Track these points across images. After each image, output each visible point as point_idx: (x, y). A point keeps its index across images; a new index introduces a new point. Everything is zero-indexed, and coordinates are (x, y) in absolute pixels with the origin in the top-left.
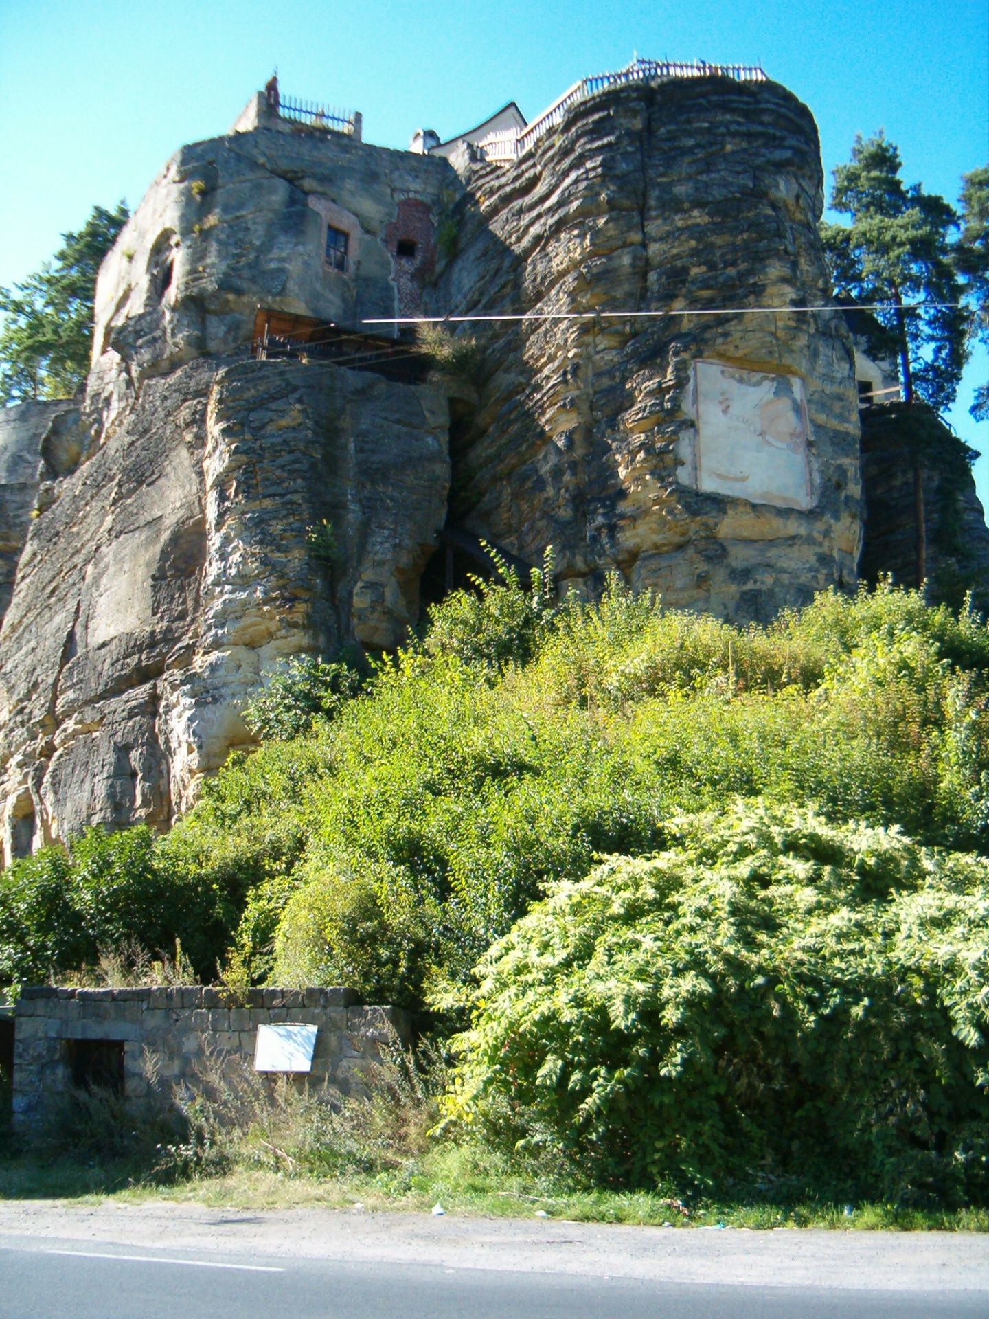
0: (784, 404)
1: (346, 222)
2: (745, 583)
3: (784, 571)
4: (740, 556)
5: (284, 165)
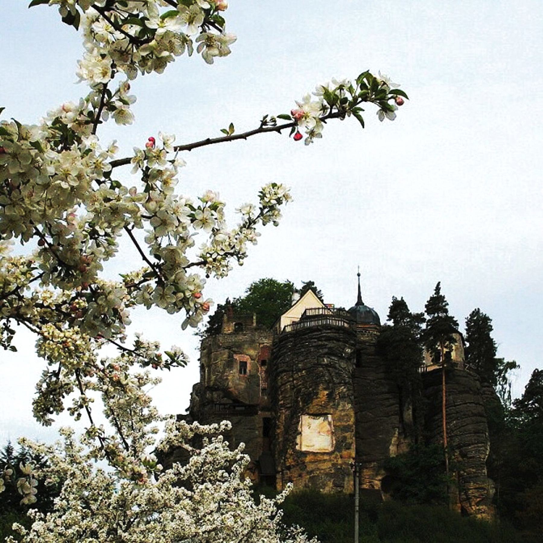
0: (326, 423)
1: (246, 358)
3: (322, 469)
4: (311, 467)
5: (227, 344)
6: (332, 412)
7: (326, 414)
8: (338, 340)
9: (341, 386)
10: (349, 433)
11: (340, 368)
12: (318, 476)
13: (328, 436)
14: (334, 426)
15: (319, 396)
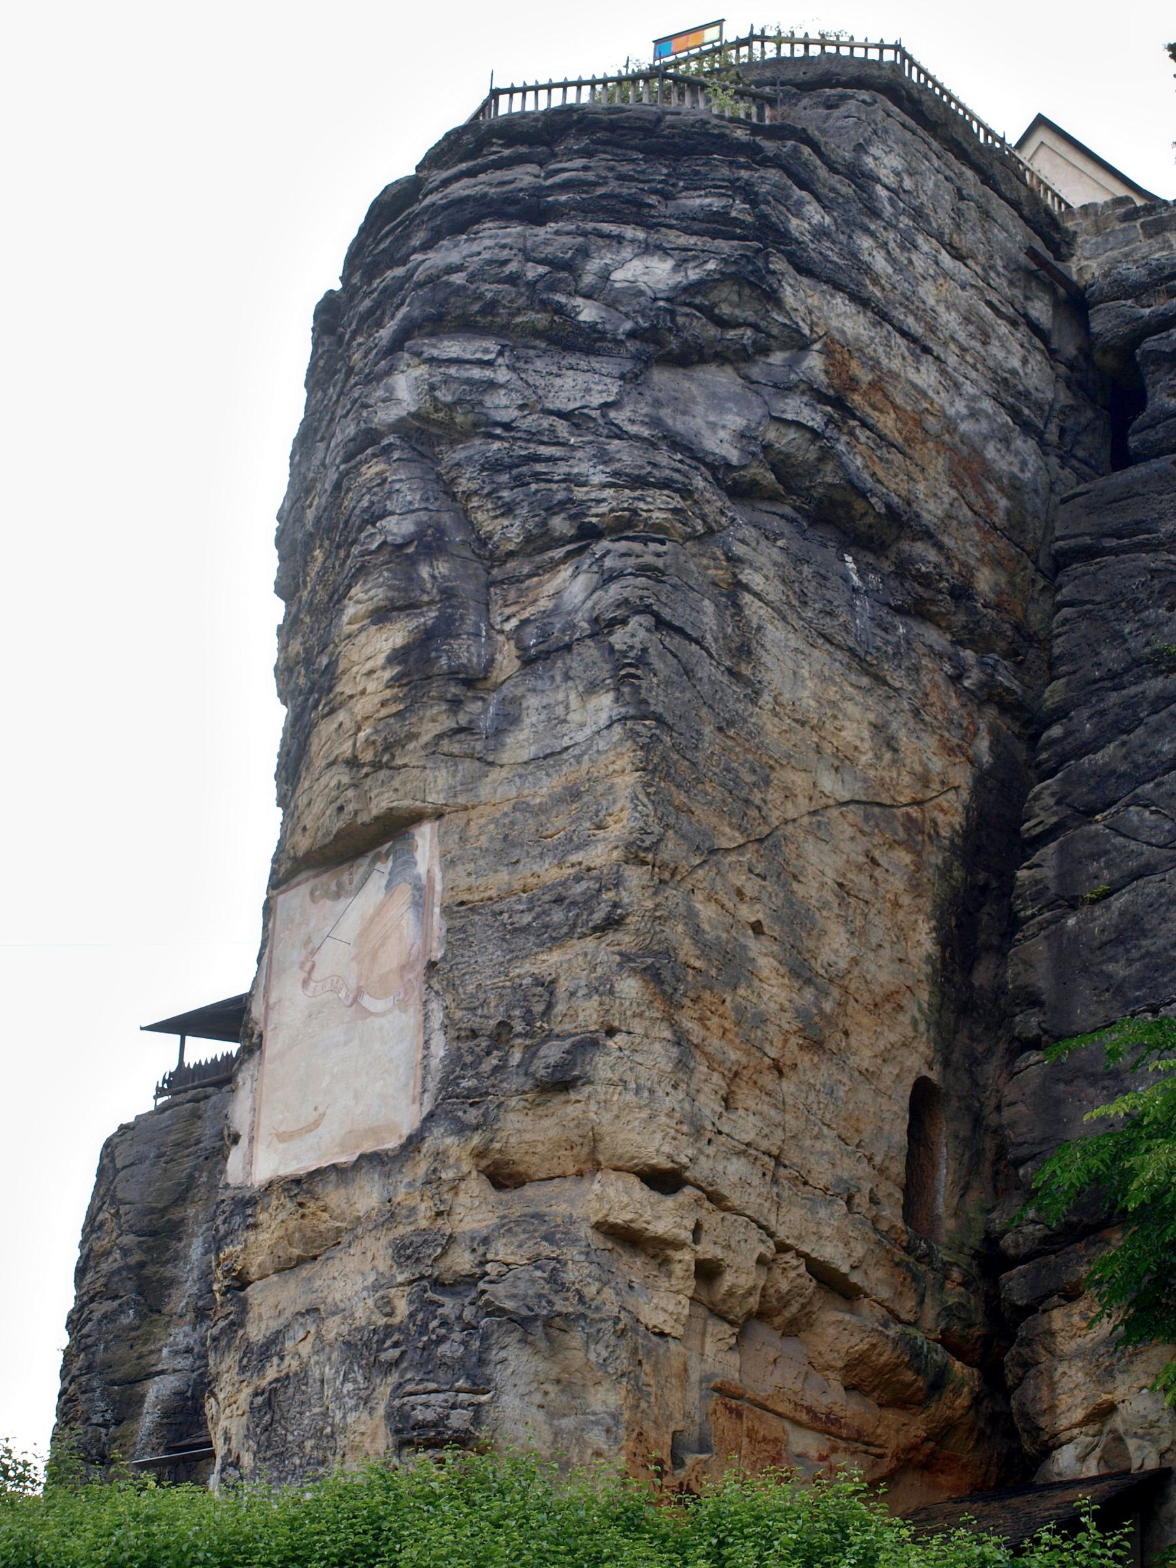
2: (261, 1370)
6: (435, 798)
7: (394, 829)
8: (532, 210)
9: (554, 565)
10: (576, 946)
11: (530, 422)
12: (302, 1377)
13: (402, 1005)
14: (447, 911)
15: (345, 687)
